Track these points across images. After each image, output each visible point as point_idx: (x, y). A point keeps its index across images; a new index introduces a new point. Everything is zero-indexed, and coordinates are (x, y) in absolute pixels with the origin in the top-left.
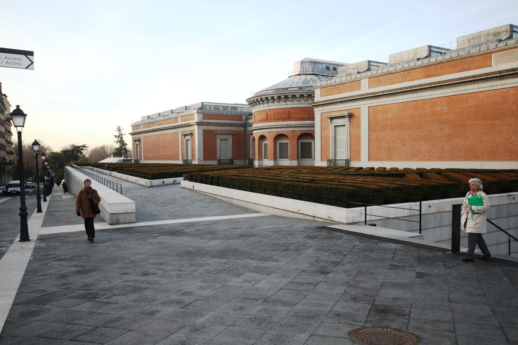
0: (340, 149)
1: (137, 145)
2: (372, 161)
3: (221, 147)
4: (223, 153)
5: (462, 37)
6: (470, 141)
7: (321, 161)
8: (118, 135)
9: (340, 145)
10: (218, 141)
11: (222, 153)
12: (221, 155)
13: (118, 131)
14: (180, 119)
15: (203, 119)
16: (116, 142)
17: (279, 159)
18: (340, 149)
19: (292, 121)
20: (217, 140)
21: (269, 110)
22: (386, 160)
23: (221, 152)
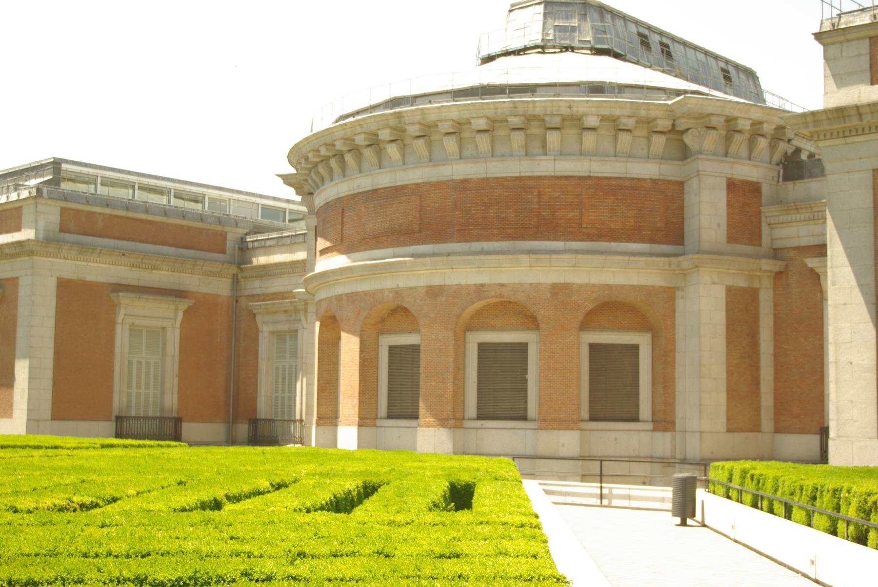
3: (130, 363)
4: (139, 387)
11: (134, 391)
12: (129, 395)
17: (479, 423)
19: (556, 239)
20: (119, 329)
21: (437, 185)
23: (129, 386)
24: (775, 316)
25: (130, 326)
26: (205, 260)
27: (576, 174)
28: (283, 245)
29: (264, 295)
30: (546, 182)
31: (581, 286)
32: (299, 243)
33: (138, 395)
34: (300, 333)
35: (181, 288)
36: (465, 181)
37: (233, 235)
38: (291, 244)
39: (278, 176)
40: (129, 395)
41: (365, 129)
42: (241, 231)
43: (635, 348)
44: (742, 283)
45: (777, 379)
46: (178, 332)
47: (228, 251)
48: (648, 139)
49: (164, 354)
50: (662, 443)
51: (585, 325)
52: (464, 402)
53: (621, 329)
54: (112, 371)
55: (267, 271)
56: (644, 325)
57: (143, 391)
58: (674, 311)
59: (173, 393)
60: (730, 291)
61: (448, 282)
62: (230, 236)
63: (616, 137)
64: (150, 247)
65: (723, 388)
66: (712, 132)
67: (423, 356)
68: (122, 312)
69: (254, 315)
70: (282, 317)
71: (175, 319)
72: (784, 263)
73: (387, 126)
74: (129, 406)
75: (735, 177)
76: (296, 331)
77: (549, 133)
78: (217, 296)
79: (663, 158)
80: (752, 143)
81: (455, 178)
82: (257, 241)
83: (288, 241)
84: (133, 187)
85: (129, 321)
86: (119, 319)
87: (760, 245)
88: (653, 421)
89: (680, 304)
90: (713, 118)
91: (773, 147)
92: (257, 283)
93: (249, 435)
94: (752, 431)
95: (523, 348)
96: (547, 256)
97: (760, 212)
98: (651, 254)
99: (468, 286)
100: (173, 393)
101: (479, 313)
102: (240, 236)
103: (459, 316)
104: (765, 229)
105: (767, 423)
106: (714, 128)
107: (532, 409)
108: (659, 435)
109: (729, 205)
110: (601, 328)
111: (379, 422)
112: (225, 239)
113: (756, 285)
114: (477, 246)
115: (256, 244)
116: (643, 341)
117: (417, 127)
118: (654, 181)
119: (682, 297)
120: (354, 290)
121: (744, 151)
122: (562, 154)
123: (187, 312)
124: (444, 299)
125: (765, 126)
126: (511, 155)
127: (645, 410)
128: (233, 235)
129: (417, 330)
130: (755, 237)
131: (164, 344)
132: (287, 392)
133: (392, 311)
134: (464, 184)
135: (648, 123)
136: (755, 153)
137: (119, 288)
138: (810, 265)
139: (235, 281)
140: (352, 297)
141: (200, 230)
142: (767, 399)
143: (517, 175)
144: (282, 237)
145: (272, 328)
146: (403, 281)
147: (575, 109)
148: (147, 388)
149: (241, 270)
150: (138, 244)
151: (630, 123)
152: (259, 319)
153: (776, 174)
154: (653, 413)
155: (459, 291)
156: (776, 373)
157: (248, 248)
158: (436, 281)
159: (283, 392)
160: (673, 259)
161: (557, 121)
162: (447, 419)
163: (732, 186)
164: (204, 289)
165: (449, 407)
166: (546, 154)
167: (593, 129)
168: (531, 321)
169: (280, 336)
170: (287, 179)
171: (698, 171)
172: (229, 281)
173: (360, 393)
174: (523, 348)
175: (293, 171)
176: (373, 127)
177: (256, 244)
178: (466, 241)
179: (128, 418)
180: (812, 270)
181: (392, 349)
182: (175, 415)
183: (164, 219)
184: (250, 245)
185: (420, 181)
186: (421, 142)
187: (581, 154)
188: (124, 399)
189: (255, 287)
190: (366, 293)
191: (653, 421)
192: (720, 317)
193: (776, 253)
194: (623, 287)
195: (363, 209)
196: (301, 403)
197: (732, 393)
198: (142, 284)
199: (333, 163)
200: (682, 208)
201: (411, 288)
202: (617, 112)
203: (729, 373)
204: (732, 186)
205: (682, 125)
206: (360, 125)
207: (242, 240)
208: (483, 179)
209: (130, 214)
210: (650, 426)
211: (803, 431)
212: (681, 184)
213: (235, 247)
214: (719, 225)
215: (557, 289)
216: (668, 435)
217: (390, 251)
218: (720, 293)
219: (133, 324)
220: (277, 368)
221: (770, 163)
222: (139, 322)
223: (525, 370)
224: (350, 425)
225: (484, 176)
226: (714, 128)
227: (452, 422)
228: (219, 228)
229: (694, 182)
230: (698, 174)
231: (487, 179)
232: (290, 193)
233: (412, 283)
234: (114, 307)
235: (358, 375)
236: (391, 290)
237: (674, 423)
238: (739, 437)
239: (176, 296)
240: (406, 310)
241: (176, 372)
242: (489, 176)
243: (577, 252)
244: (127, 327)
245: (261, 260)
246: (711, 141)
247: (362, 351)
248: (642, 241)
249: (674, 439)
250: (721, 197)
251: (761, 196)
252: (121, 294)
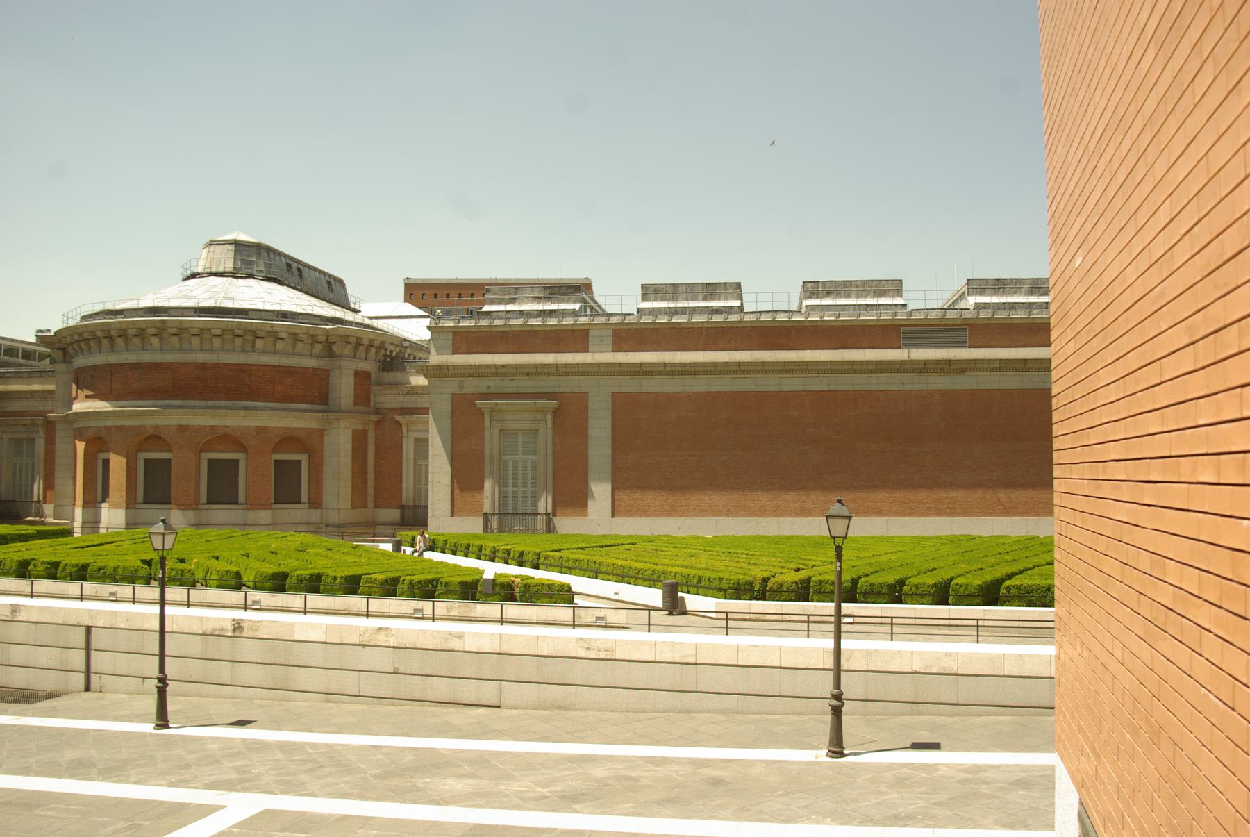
0: (515, 485)
2: (622, 516)
5: (814, 282)
6: (863, 481)
7: (452, 515)
9: (515, 477)
18: (515, 485)
21: (186, 365)
22: (663, 515)
24: (376, 445)
27: (271, 364)
30: (254, 367)
31: (273, 428)
36: (204, 364)
41: (137, 326)
43: (300, 462)
44: (360, 427)
45: (376, 479)
48: (312, 345)
50: (315, 515)
51: (275, 450)
53: (291, 452)
56: (305, 450)
58: (323, 442)
60: (354, 431)
61: (192, 424)
63: (294, 344)
65: (350, 485)
66: (349, 345)
72: (381, 416)
73: (152, 327)
75: (359, 369)
76: (34, 439)
77: (257, 340)
79: (319, 357)
80: (367, 351)
81: (198, 361)
87: (369, 406)
88: (309, 503)
89: (327, 439)
90: (351, 338)
91: (377, 352)
94: (363, 508)
95: (236, 462)
96: (256, 411)
97: (369, 388)
98: (312, 411)
99: (205, 426)
101: (208, 442)
104: (372, 397)
105: (371, 504)
106: (350, 343)
107: (242, 498)
108: (313, 511)
109: (355, 385)
110: (281, 451)
113: (367, 428)
114: (211, 403)
116: (304, 458)
117: (175, 330)
118: (314, 369)
119: (328, 434)
121: (363, 355)
122: (264, 352)
125: (376, 342)
126: (234, 351)
127: (304, 498)
129: (170, 451)
130: (367, 401)
133: (147, 437)
134: (203, 366)
135: (314, 339)
136: (369, 356)
138: (397, 419)
140: (120, 429)
142: (371, 491)
143: (237, 362)
144: (19, 372)
145: (11, 436)
146: (161, 421)
147: (274, 328)
151: (304, 337)
153: (378, 367)
154: (309, 499)
155: (199, 429)
156: (375, 476)
158: (184, 422)
159: (20, 481)
160: (325, 414)
161: (263, 334)
163: (357, 374)
166: (254, 352)
167: (283, 339)
168: (242, 448)
171: (340, 366)
173: (127, 488)
174: (236, 462)
176: (143, 326)
178: (204, 400)
180: (397, 421)
181: (147, 461)
185: (173, 361)
186: (175, 339)
187: (274, 353)
191: (309, 503)
192: (349, 446)
193: (377, 411)
194: (296, 428)
195: (130, 374)
196: (39, 490)
197: (354, 488)
199: (105, 342)
200: (328, 384)
201: (166, 426)
202: (298, 331)
203: (353, 477)
204: (357, 374)
205: (333, 339)
206: (134, 324)
208: (216, 364)
210: (307, 506)
211: (390, 507)
212: (328, 371)
214: (350, 396)
215: (259, 430)
216: (319, 510)
218: (349, 433)
220: (15, 464)
221: (375, 361)
223: (237, 475)
224: (119, 508)
225: (217, 362)
226: (350, 343)
229: (338, 372)
230: (340, 367)
231: (218, 363)
235: (125, 477)
236: (152, 426)
237: (322, 504)
238: (357, 511)
240: (158, 437)
242: (220, 362)
243: (272, 409)
246: (348, 350)
247: (127, 463)
248: (307, 403)
249: (322, 513)
250: (352, 380)
251: (370, 380)
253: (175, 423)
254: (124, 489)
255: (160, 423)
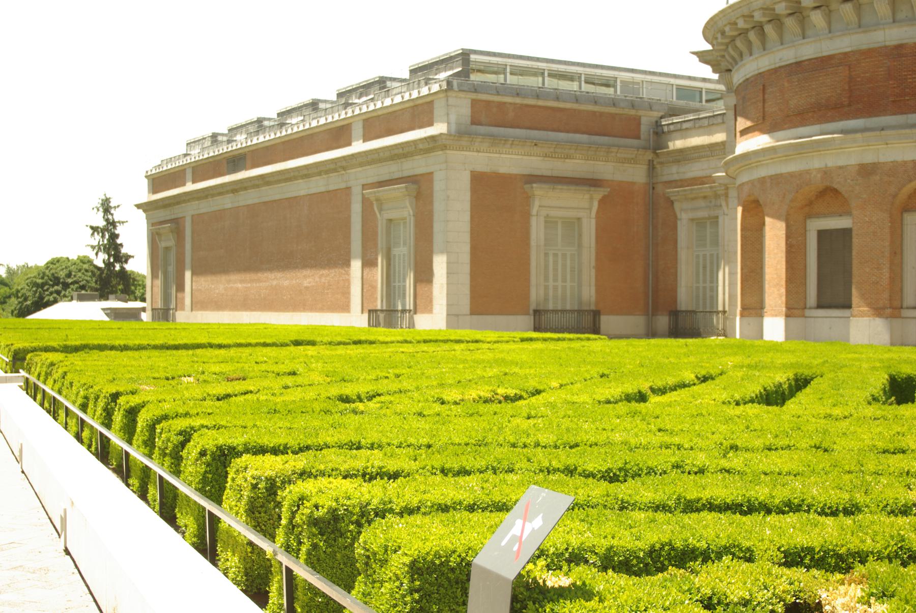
1: (167, 249)
4: (555, 280)
8: (101, 223)
10: (537, 230)
11: (551, 283)
12: (546, 288)
13: (101, 209)
14: (357, 130)
15: (474, 122)
16: (93, 247)
20: (534, 221)
23: (546, 279)
25: (545, 217)
26: (619, 146)
28: (700, 127)
29: (681, 180)
32: (717, 124)
33: (555, 288)
34: (720, 220)
35: (596, 177)
37: (647, 119)
38: (709, 125)
39: (693, 53)
40: (546, 288)
42: (656, 114)
46: (593, 222)
47: (642, 137)
49: (580, 245)
52: (902, 290)
54: (529, 264)
55: (684, 155)
57: (560, 283)
59: (590, 286)
62: (644, 120)
64: (562, 136)
67: (855, 241)
68: (537, 204)
69: (672, 202)
70: (702, 203)
71: (590, 209)
74: (546, 300)
78: (633, 183)
82: (673, 124)
83: (706, 122)
84: (543, 74)
85: (544, 212)
86: (534, 211)
92: (674, 169)
93: (669, 328)
100: (590, 286)
102: (654, 120)
103: (895, 196)
111: (808, 313)
112: (639, 124)
115: (672, 128)
120: (778, 172)
123: (602, 202)
124: (878, 178)
128: (647, 119)
129: (848, 213)
131: (580, 235)
132: (708, 282)
133: (821, 192)
137: (533, 179)
139: (651, 167)
140: (776, 179)
141: (613, 116)
144: (699, 119)
145: (691, 215)
146: (832, 161)
148: (564, 280)
149: (657, 155)
150: (550, 133)
152: (677, 206)
157: (663, 132)
158: (869, 158)
159: (705, 282)
162: (884, 308)
164: (618, 177)
165: (886, 295)
169: (700, 223)
170: (703, 57)
172: (645, 167)
175: (708, 47)
177: (672, 128)
179: (546, 311)
181: (822, 234)
182: (593, 307)
183: (575, 106)
184: (666, 129)
188: (542, 292)
189: (673, 172)
190: (791, 175)
195: (786, 84)
196: (724, 294)
198: (555, 174)
201: (841, 168)
207: (657, 124)
209: (541, 103)
213: (649, 131)
217: (816, 128)
219: (548, 215)
220: (698, 256)
222: (554, 213)
227: (889, 311)
228: (633, 112)
232: (706, 71)
233: (841, 163)
234: (528, 199)
235: (784, 263)
236: (819, 170)
239: (591, 186)
240: (836, 192)
241: (593, 263)
244: (542, 219)
245: (678, 144)
247: (788, 237)
252: (534, 185)
253: (853, 161)
254: (783, 283)
255: (830, 164)
